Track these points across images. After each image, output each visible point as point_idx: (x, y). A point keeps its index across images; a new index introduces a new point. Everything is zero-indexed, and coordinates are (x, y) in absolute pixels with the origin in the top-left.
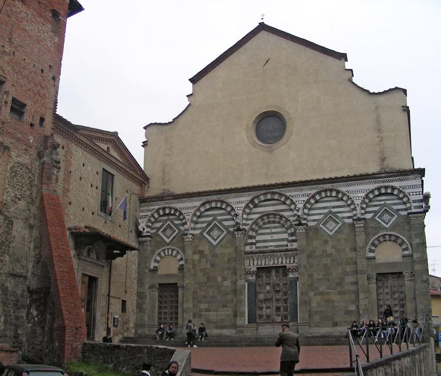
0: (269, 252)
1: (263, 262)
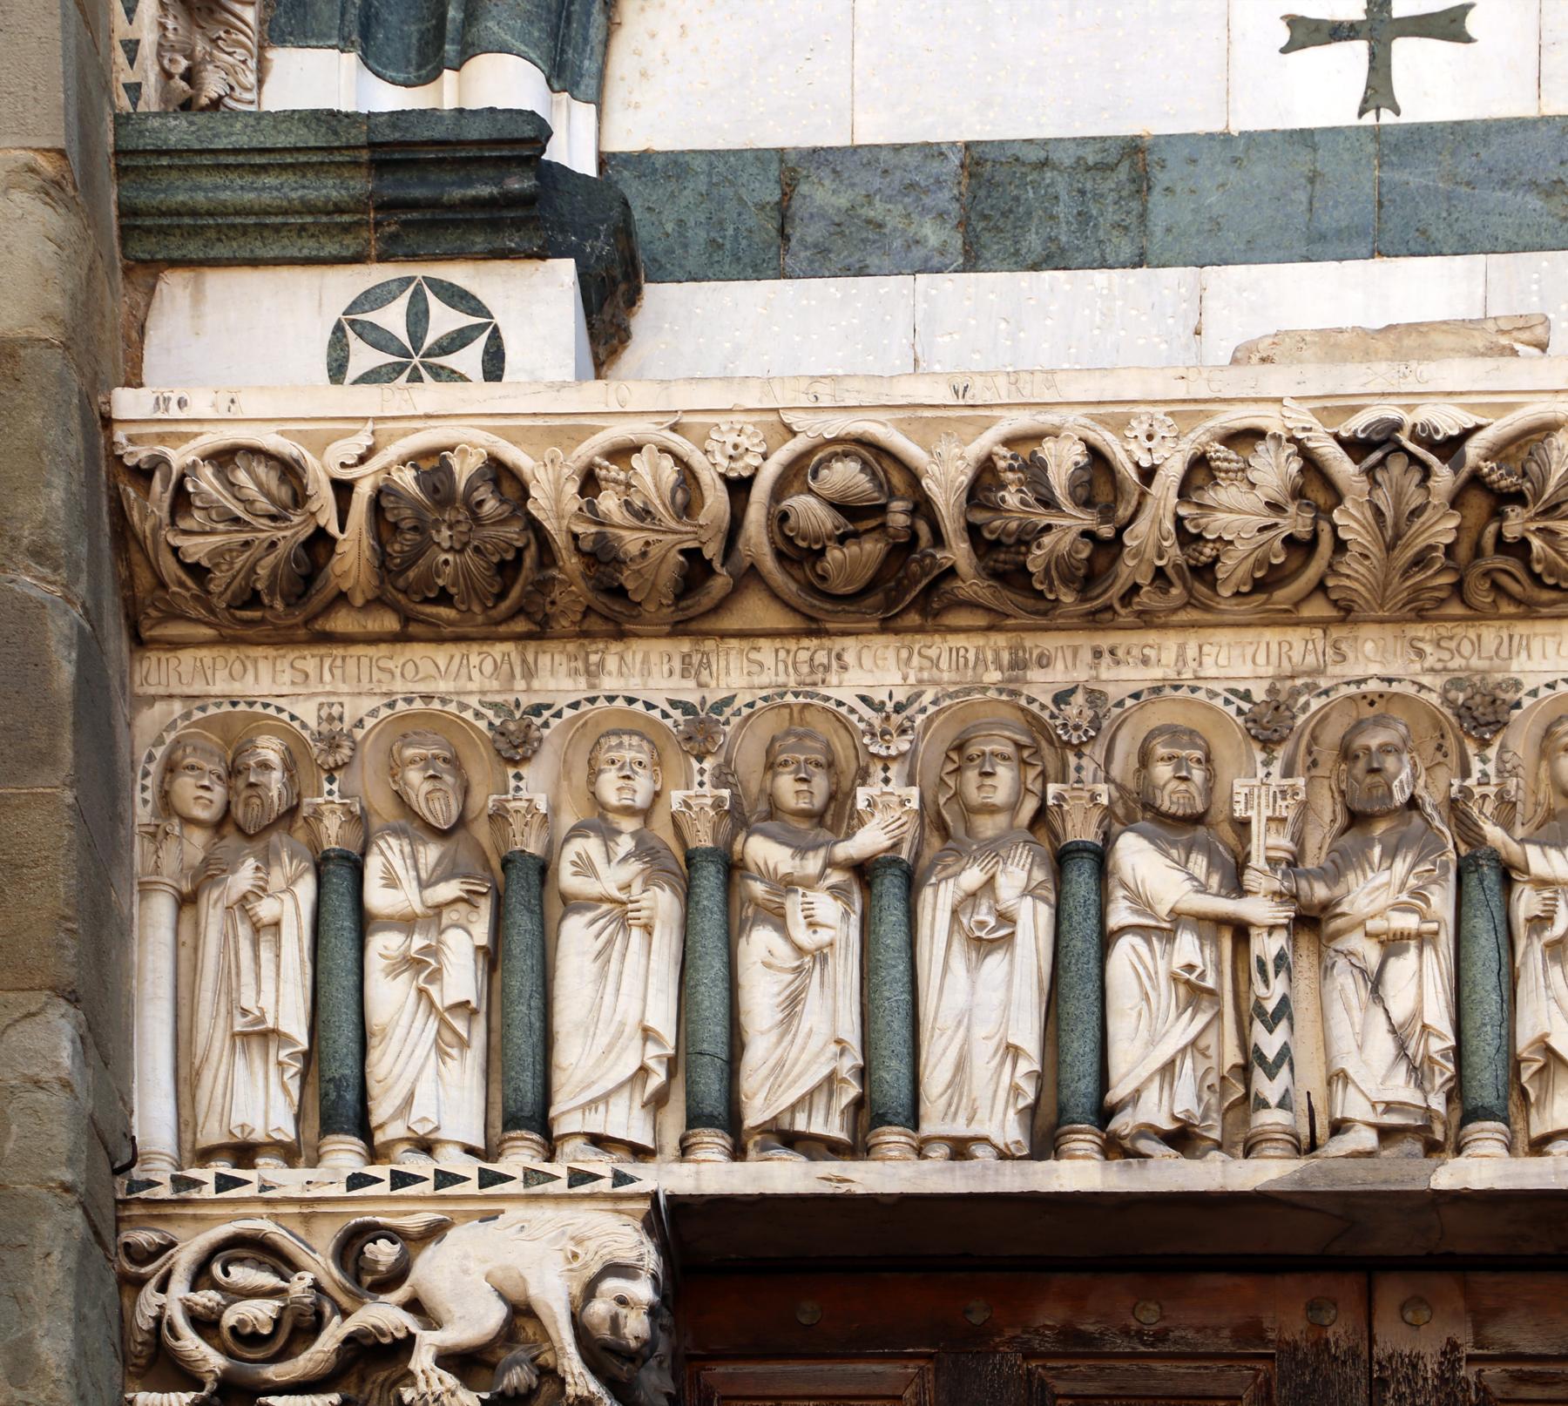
1: (982, 1015)
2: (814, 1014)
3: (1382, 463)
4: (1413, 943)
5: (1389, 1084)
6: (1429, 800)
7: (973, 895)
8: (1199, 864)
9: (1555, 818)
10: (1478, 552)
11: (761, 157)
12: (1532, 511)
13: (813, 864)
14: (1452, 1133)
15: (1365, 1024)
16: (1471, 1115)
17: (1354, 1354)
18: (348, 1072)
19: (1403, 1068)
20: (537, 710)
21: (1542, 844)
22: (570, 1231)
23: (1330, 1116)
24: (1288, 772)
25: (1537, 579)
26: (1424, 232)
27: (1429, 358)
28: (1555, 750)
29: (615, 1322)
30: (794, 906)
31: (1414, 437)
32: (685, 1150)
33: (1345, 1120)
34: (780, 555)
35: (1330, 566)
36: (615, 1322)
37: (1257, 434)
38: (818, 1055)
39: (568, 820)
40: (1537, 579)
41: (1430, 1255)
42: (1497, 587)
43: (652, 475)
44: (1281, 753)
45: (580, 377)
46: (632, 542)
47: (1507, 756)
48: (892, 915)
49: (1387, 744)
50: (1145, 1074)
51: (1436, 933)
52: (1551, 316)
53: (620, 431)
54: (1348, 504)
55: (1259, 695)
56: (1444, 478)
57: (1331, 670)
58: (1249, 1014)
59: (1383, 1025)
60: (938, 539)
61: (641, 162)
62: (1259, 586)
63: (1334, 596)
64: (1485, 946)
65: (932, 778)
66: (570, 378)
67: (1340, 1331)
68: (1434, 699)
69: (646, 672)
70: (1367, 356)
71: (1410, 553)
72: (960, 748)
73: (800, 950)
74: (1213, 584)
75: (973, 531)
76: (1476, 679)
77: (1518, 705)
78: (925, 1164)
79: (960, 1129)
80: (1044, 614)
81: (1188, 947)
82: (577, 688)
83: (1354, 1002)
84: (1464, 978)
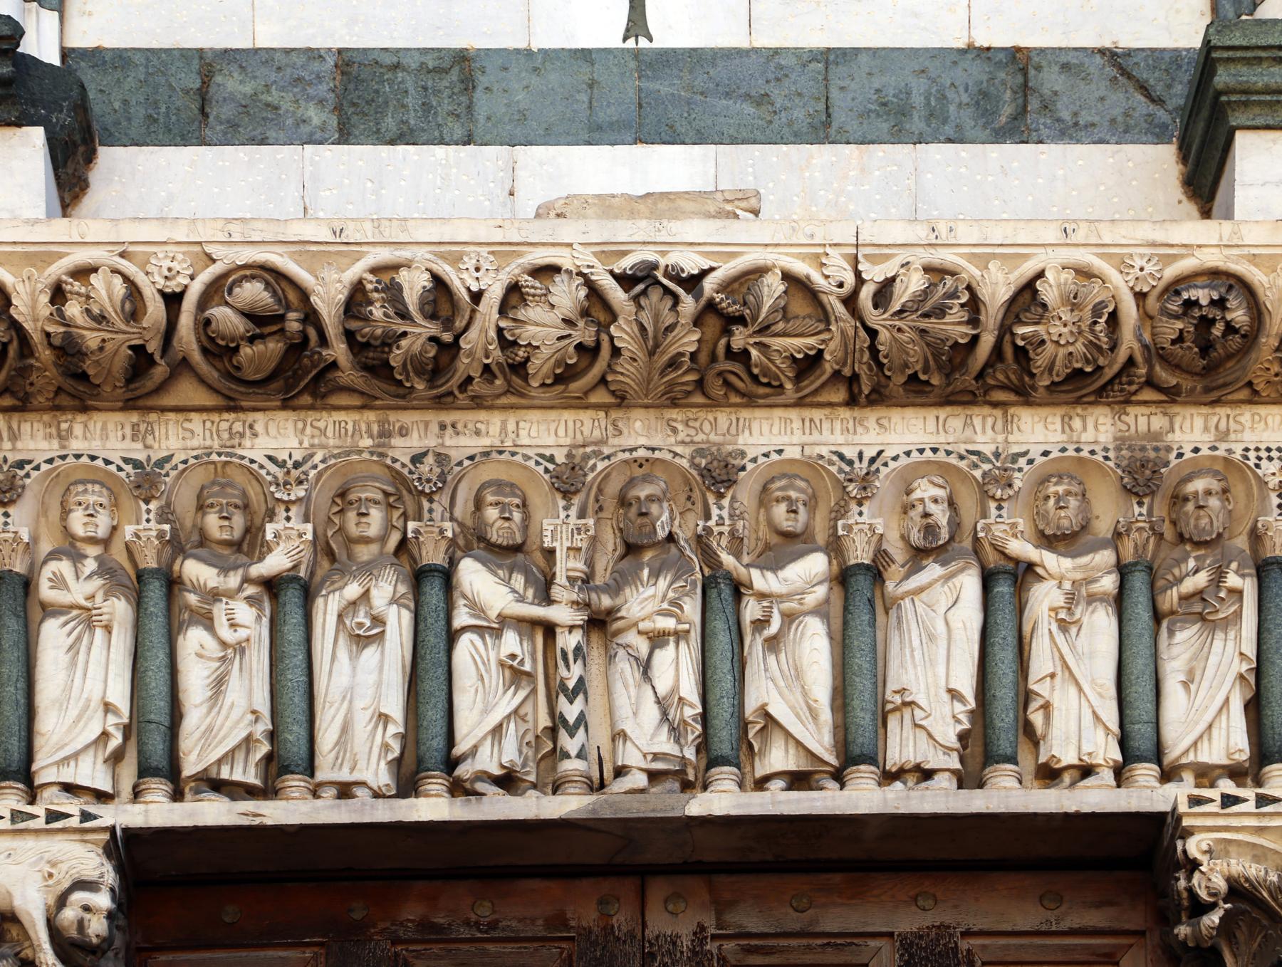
0: (582, 373)
1: (361, 693)
2: (235, 692)
3: (644, 293)
4: (671, 638)
5: (655, 740)
6: (683, 535)
7: (354, 604)
8: (518, 581)
9: (770, 549)
10: (713, 358)
11: (186, 55)
12: (751, 329)
13: (234, 580)
14: (700, 776)
15: (638, 697)
16: (713, 762)
17: (631, 935)
19: (665, 728)
20: (21, 464)
21: (762, 568)
22: (47, 856)
23: (614, 763)
24: (582, 515)
25: (755, 378)
26: (672, 127)
27: (676, 218)
28: (770, 501)
29: (81, 924)
30: (219, 611)
31: (667, 274)
32: (137, 794)
33: (624, 767)
34: (205, 351)
35: (609, 366)
36: (81, 924)
37: (553, 270)
38: (238, 722)
39: (45, 547)
40: (755, 378)
41: (685, 863)
42: (727, 384)
43: (107, 290)
44: (576, 500)
45: (50, 215)
46: (92, 339)
47: (736, 505)
48: (294, 618)
49: (651, 495)
50: (481, 735)
51: (688, 631)
52: (762, 191)
53: (81, 257)
54: (621, 321)
55: (560, 459)
56: (688, 305)
57: (611, 441)
58: (556, 690)
59: (653, 698)
60: (324, 341)
61: (95, 55)
62: (559, 380)
63: (612, 388)
64: (722, 641)
65: (322, 517)
66: (42, 216)
67: (622, 919)
68: (685, 463)
69: (105, 436)
70: (633, 215)
71: (666, 358)
72: (343, 494)
73: (224, 645)
74: (525, 378)
75: (349, 335)
76: (714, 449)
77: (743, 468)
78: (319, 802)
79: (344, 775)
80: (402, 397)
81: (511, 642)
82: (50, 448)
83: (631, 681)
84: (708, 663)
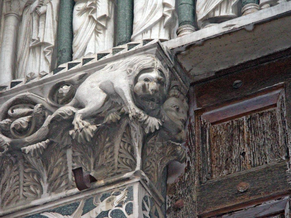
18: (65, 47)
29: (144, 87)
